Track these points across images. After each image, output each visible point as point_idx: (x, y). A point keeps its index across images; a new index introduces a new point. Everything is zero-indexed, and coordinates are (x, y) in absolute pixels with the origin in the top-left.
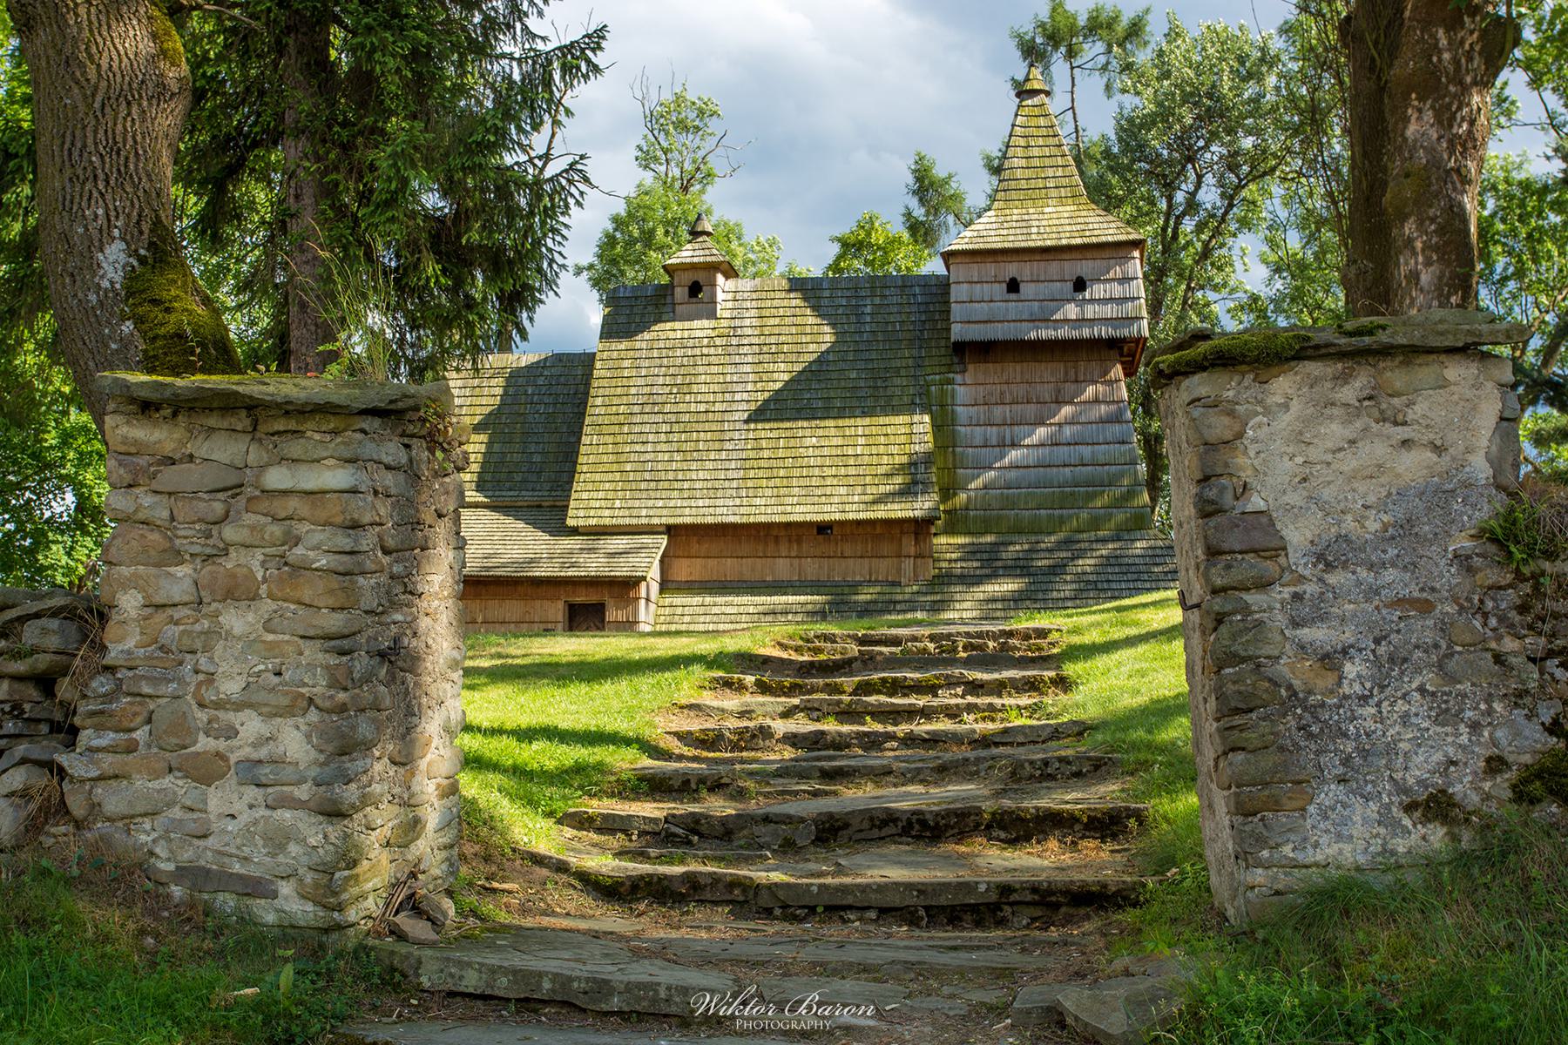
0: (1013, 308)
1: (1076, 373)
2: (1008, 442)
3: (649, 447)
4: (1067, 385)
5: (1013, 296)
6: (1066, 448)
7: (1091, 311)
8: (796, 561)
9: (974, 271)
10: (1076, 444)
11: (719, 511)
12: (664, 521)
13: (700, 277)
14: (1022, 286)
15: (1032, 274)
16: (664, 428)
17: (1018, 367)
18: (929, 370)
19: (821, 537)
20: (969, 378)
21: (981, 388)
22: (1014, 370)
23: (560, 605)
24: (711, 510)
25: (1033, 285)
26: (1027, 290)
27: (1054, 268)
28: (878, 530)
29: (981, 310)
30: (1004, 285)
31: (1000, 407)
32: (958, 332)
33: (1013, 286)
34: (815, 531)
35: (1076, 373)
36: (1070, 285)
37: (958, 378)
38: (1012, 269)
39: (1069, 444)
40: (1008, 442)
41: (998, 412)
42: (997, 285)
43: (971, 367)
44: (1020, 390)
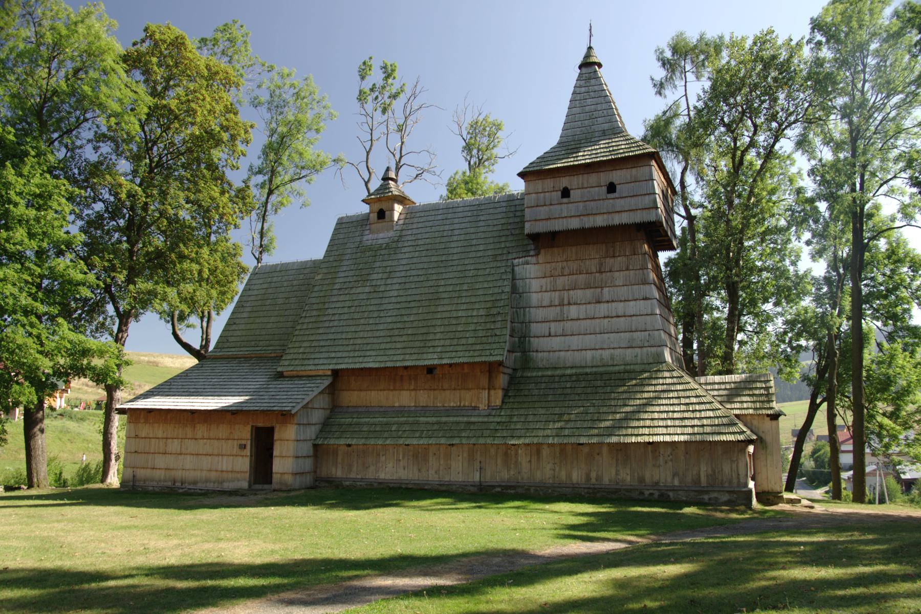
0: (566, 209)
1: (614, 251)
2: (566, 302)
3: (336, 317)
4: (608, 260)
5: (565, 200)
6: (606, 305)
8: (413, 393)
9: (539, 185)
10: (613, 301)
11: (366, 359)
13: (384, 206)
14: (572, 192)
15: (578, 184)
16: (348, 304)
17: (574, 249)
18: (515, 255)
19: (429, 376)
20: (541, 258)
21: (548, 265)
23: (249, 428)
24: (361, 360)
25: (579, 190)
27: (593, 178)
28: (466, 371)
29: (543, 212)
30: (560, 193)
31: (562, 278)
32: (528, 228)
33: (566, 193)
34: (425, 372)
35: (614, 251)
36: (605, 189)
37: (533, 260)
38: (564, 182)
39: (608, 302)
40: (566, 302)
41: (561, 281)
42: (555, 193)
43: (542, 251)
44: (574, 266)
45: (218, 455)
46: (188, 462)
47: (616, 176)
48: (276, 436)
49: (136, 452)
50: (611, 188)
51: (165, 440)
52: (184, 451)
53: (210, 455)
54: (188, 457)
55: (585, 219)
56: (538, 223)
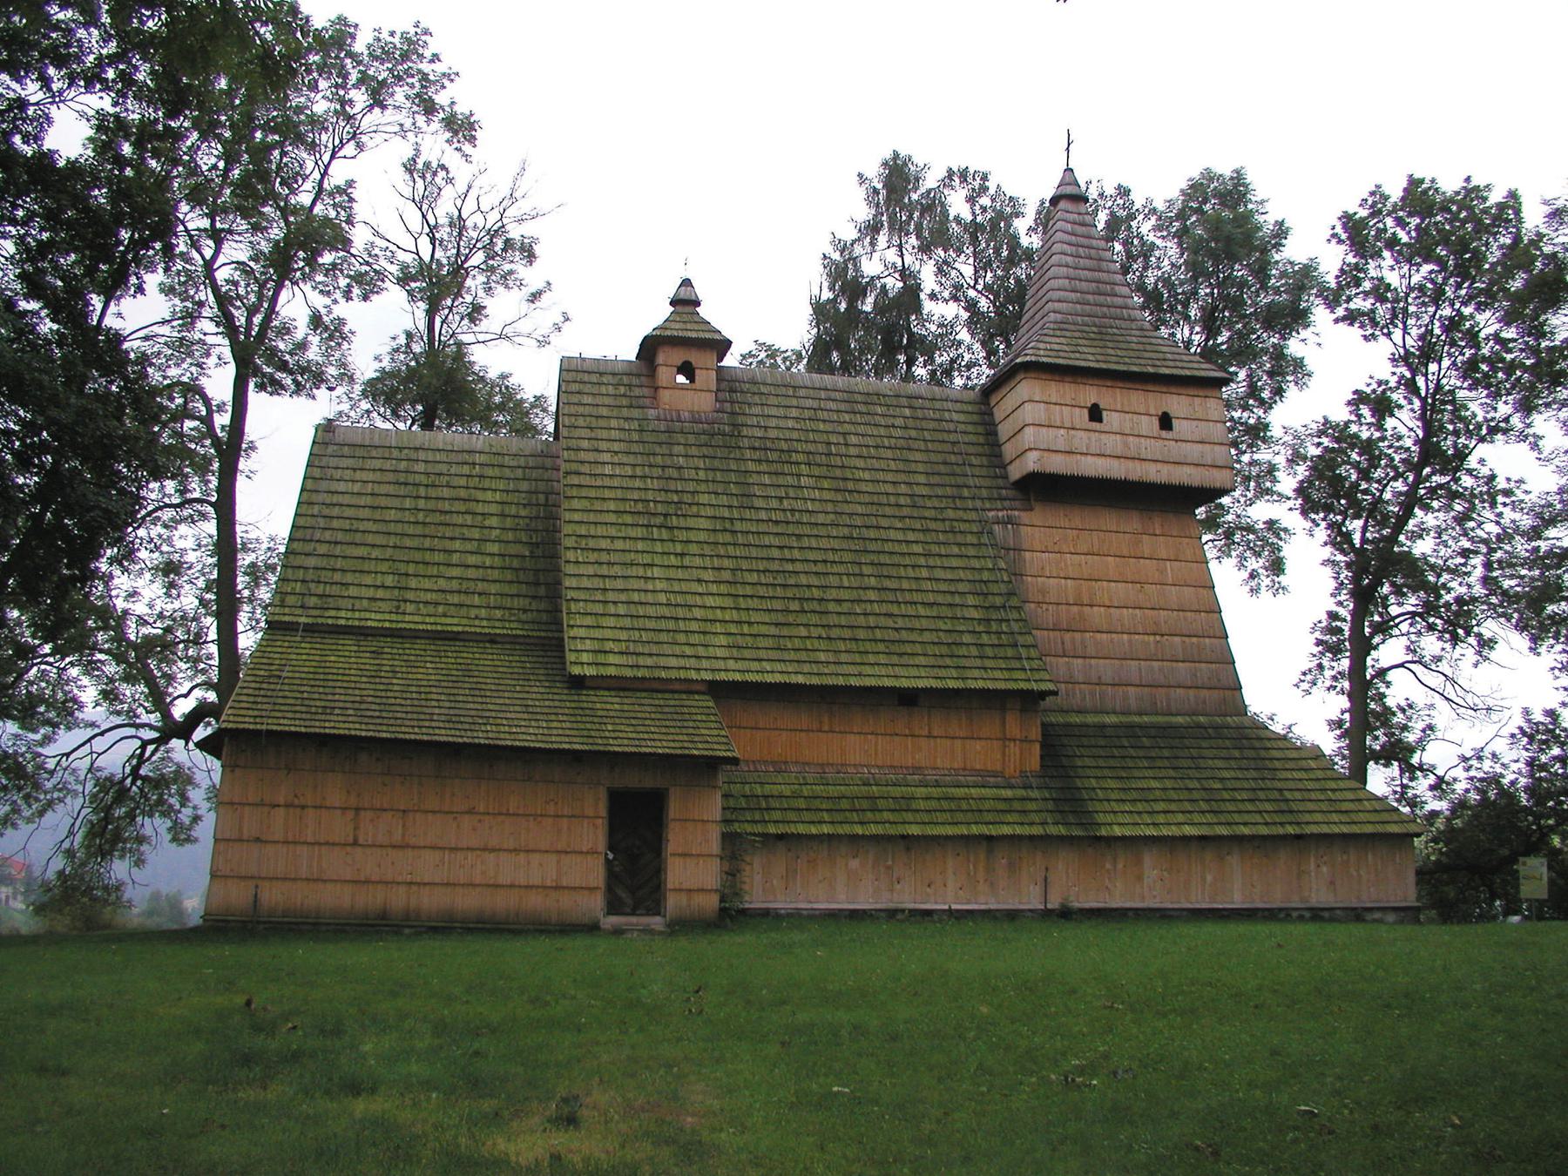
7: (1177, 451)
12: (708, 676)
22: (1108, 520)
26: (1111, 419)
27: (1137, 399)
30: (1086, 412)
33: (1095, 414)
36: (1156, 422)
38: (1090, 394)
45: (516, 851)
46: (427, 866)
47: (1176, 403)
48: (674, 808)
49: (258, 840)
50: (1166, 422)
51: (351, 814)
52: (413, 841)
53: (493, 850)
54: (427, 854)
55: (1130, 464)
56: (1054, 456)
